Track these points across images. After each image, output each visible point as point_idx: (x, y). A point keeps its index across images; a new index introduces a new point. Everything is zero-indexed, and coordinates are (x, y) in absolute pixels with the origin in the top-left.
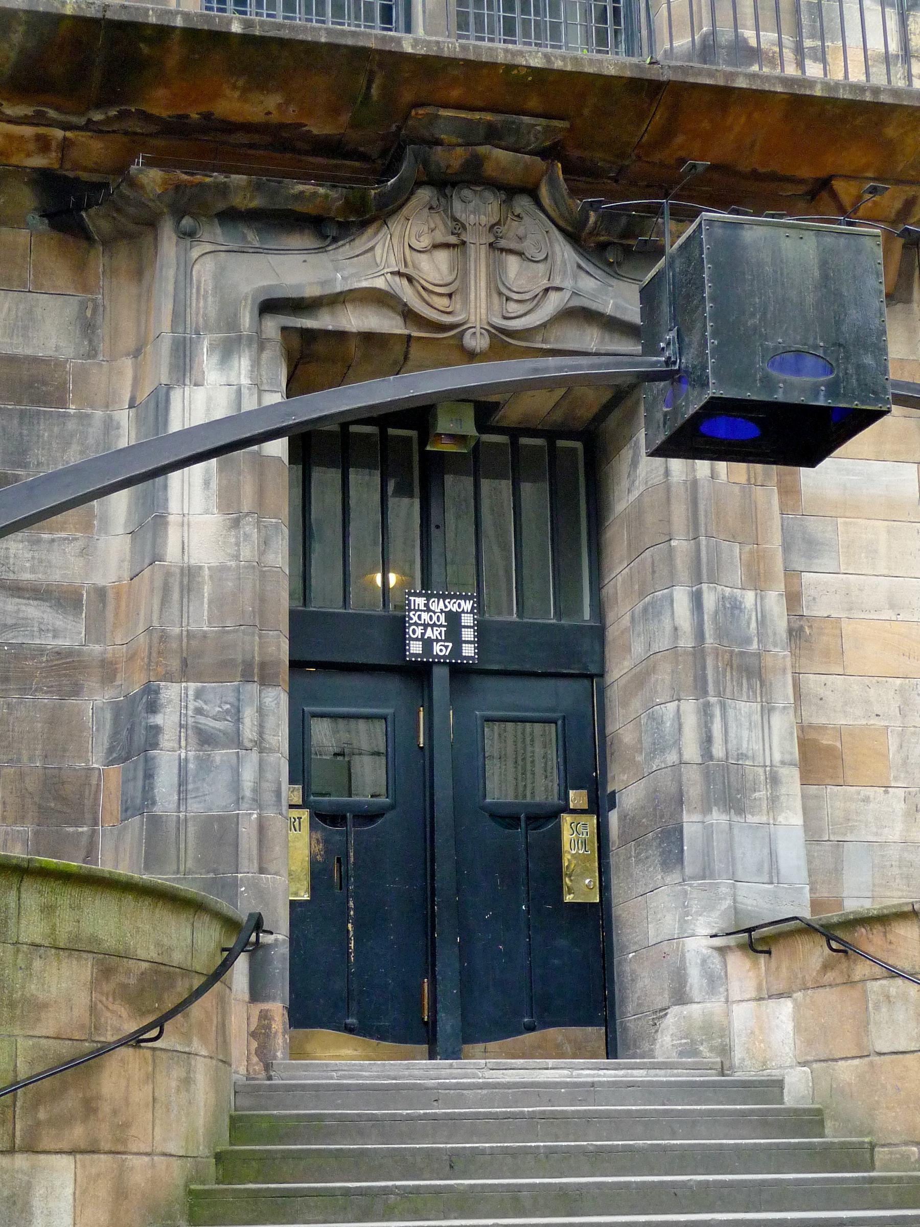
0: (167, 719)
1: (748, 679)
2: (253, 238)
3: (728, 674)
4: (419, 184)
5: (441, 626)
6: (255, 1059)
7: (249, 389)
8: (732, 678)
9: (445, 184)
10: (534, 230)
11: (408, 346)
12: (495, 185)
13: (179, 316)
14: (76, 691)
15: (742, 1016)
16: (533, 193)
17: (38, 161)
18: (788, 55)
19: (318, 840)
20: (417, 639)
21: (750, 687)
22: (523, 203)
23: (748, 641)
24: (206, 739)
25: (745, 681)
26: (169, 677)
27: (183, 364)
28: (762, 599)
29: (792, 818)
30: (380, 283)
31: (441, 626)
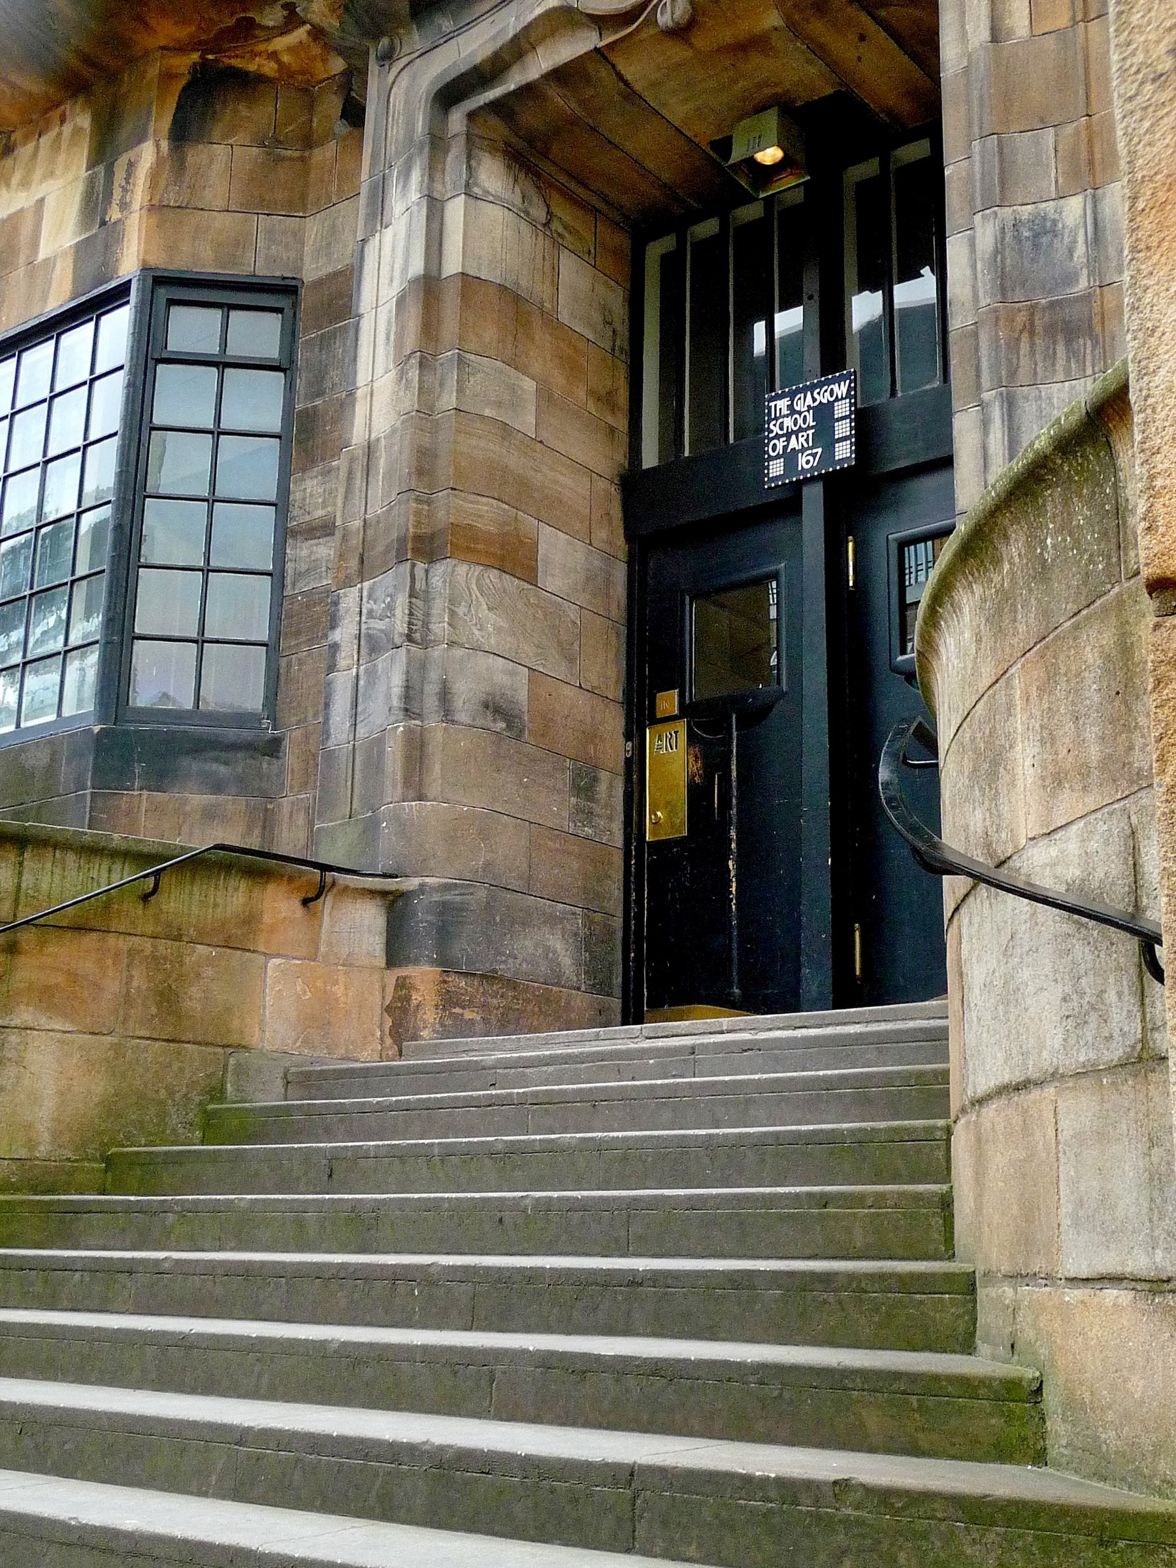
1: (1068, 342)
2: (447, 24)
3: (1024, 347)
5: (809, 428)
6: (389, 1041)
7: (418, 204)
8: (1033, 352)
11: (613, 66)
19: (696, 757)
20: (778, 457)
21: (1071, 353)
23: (1070, 279)
25: (1061, 349)
28: (1095, 201)
31: (809, 428)
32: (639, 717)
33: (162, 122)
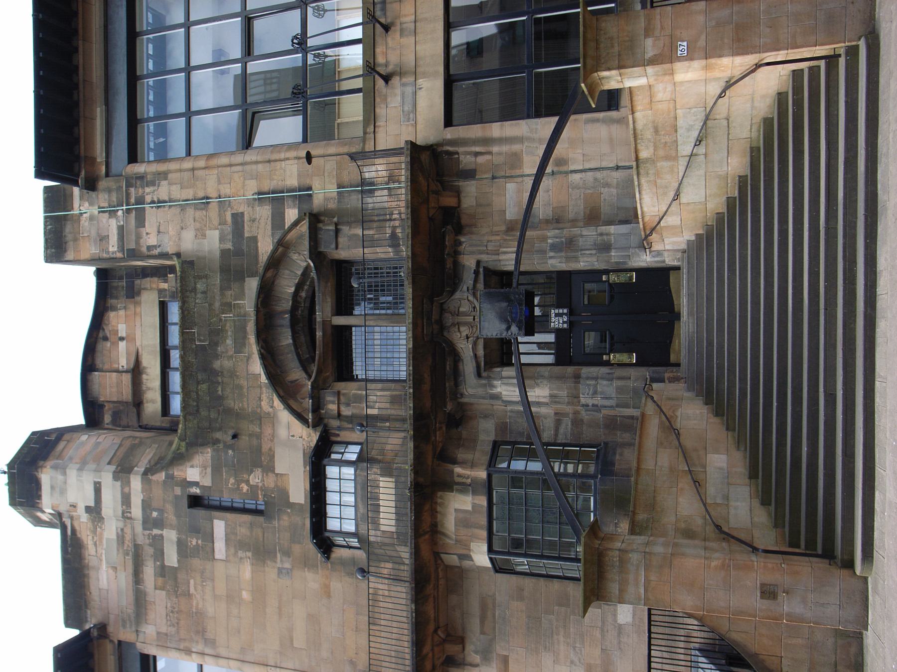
0: (590, 402)
4: (443, 335)
9: (442, 328)
10: (452, 304)
12: (441, 314)
13: (484, 398)
14: (582, 420)
16: (442, 304)
17: (444, 429)
18: (392, 223)
22: (445, 306)
24: (595, 393)
26: (579, 402)
27: (497, 397)
29: (612, 229)
32: (608, 364)
33: (450, 466)
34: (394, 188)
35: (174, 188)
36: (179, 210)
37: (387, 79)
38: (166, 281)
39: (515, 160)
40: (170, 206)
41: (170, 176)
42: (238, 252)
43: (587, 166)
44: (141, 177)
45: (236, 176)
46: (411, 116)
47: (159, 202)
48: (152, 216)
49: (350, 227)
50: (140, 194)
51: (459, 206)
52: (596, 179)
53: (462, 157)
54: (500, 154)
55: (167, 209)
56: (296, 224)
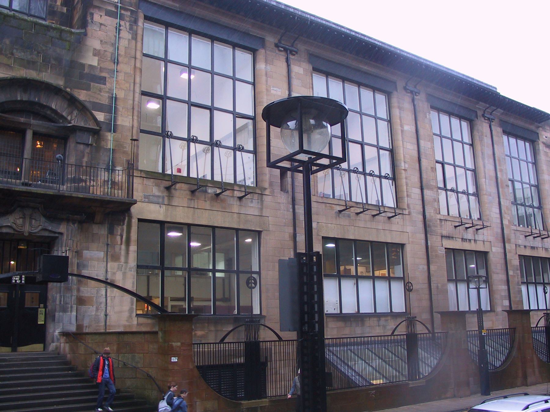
15: (62, 345)
16: (38, 209)
29: (74, 313)
30: (9, 224)
34: (108, 184)
35: (127, 42)
36: (113, 42)
37: (168, 189)
38: (62, 5)
39: (116, 258)
40: (116, 36)
41: (134, 42)
42: (82, 76)
43: (109, 299)
44: (136, 22)
45: (128, 85)
46: (147, 200)
47: (120, 30)
48: (111, 22)
49: (88, 153)
50: (126, 18)
51: (93, 223)
52: (101, 303)
53: (120, 227)
54: (120, 249)
55: (115, 34)
56: (95, 119)
